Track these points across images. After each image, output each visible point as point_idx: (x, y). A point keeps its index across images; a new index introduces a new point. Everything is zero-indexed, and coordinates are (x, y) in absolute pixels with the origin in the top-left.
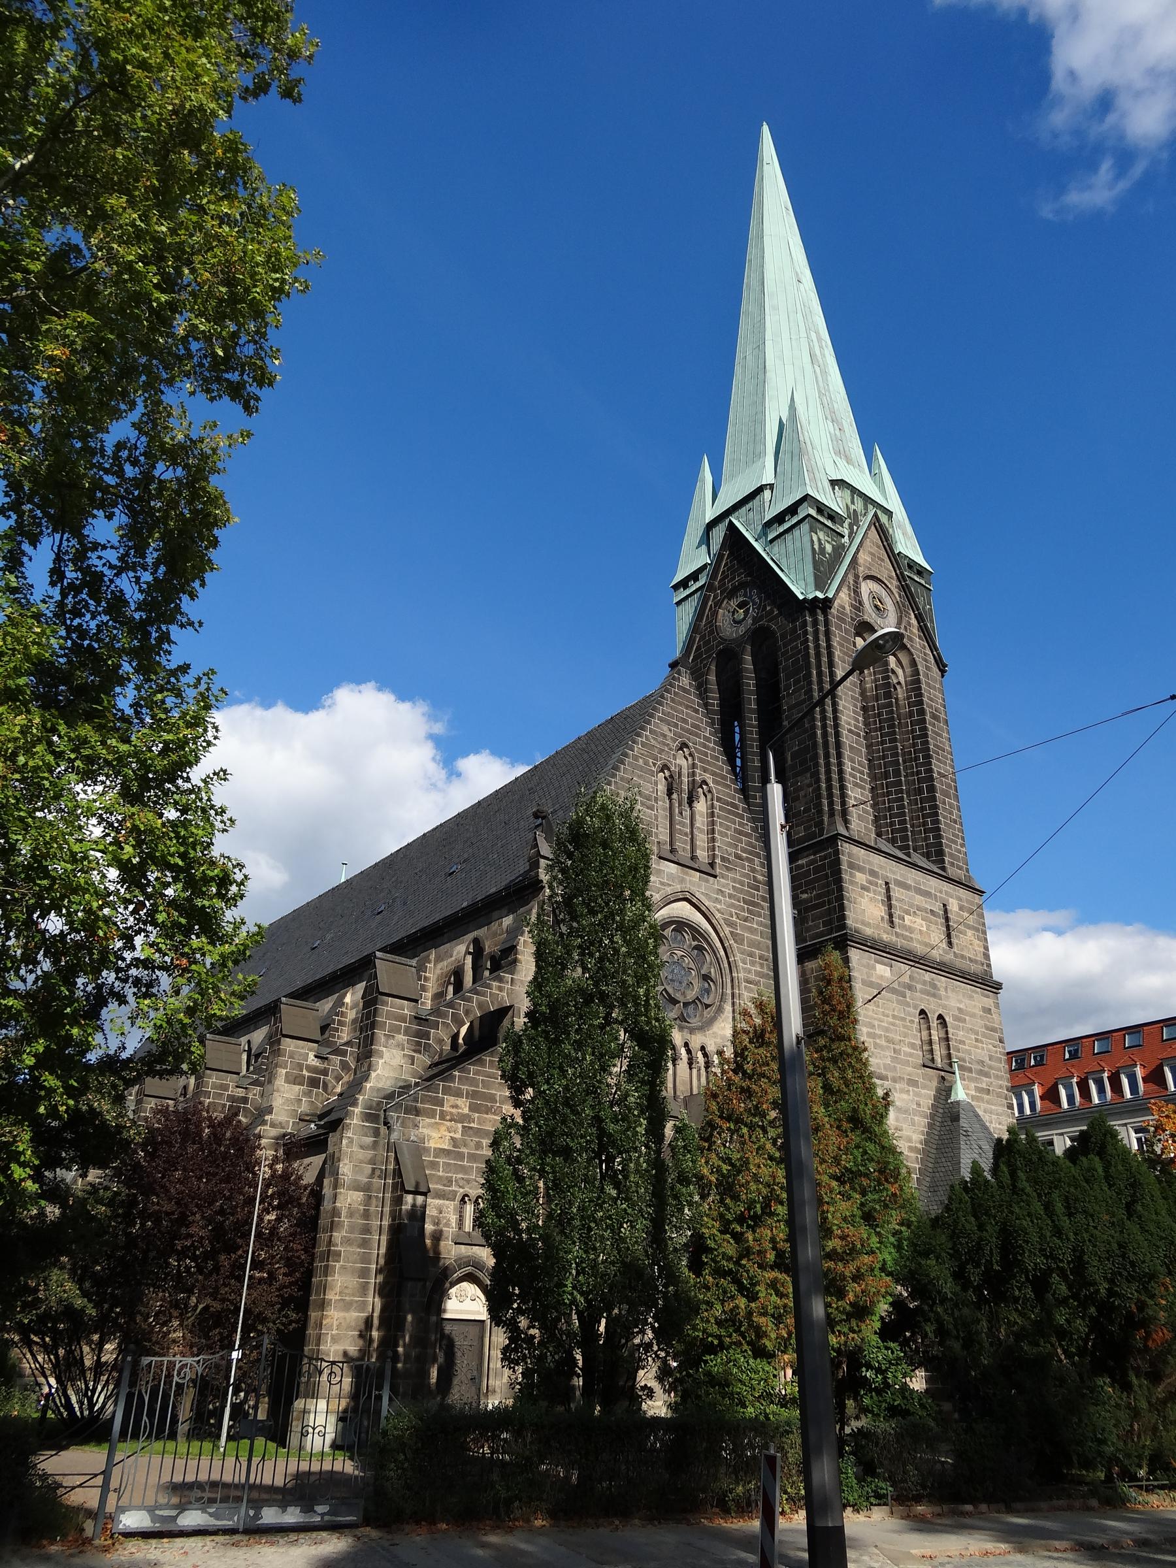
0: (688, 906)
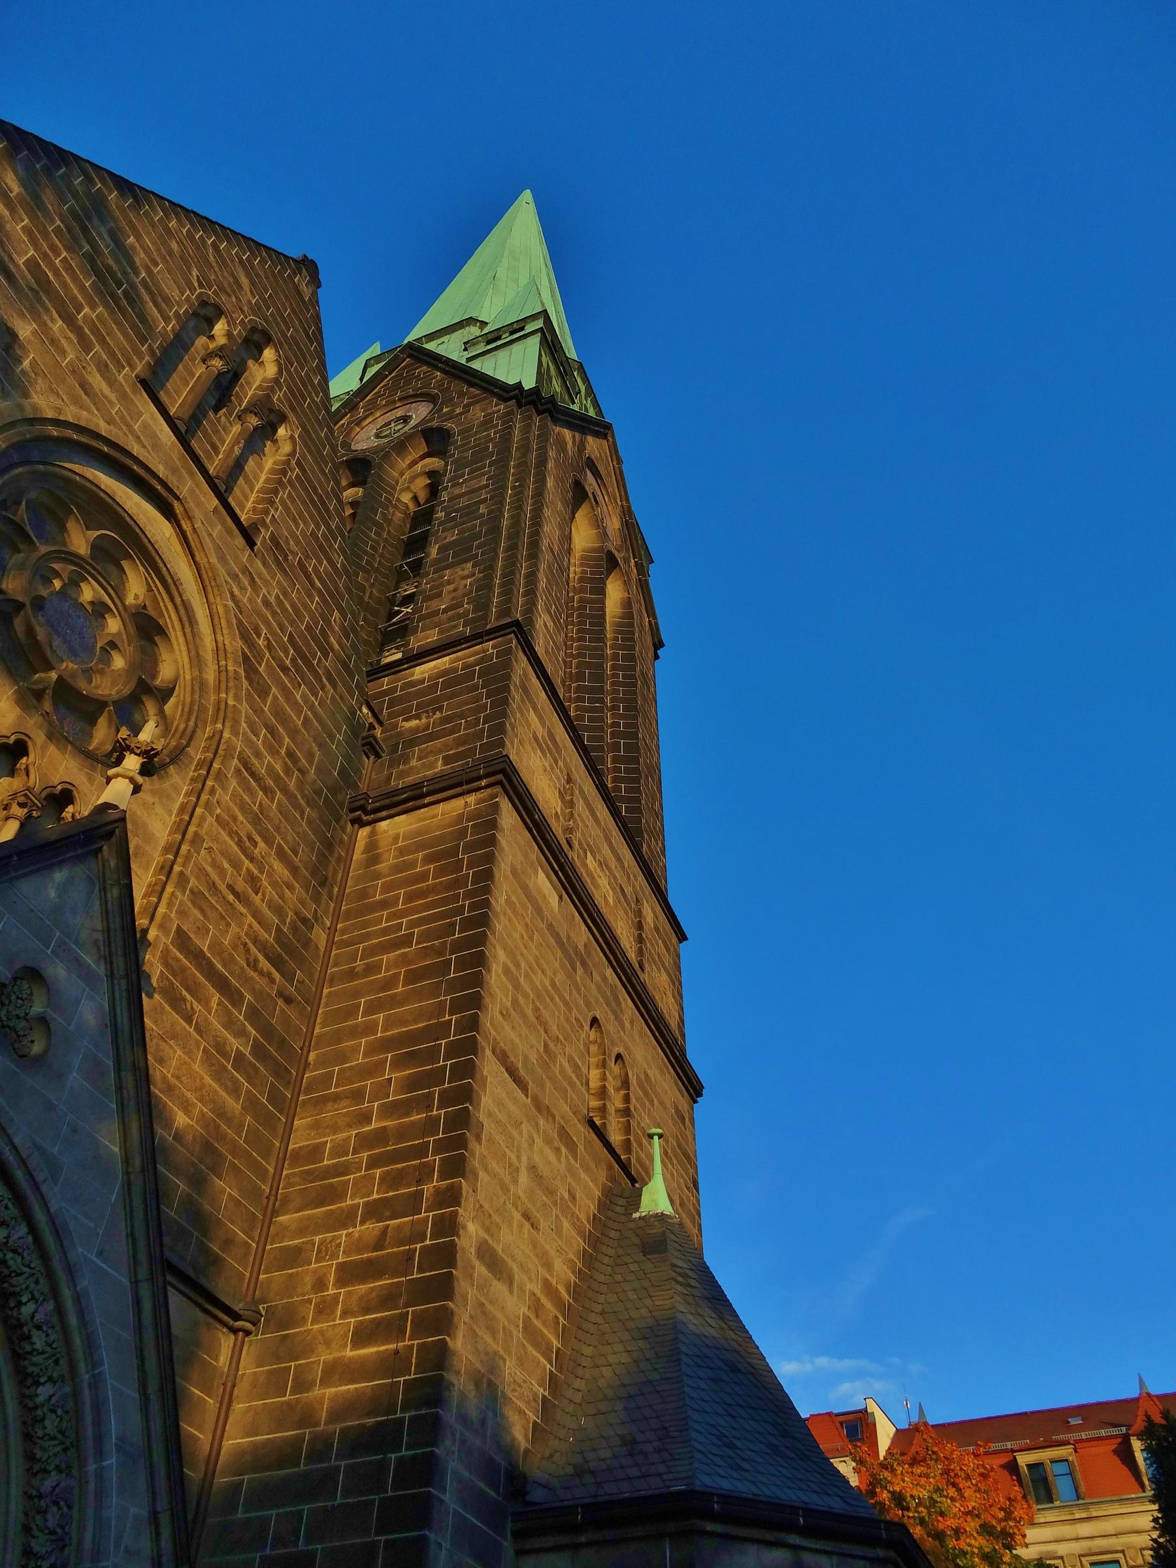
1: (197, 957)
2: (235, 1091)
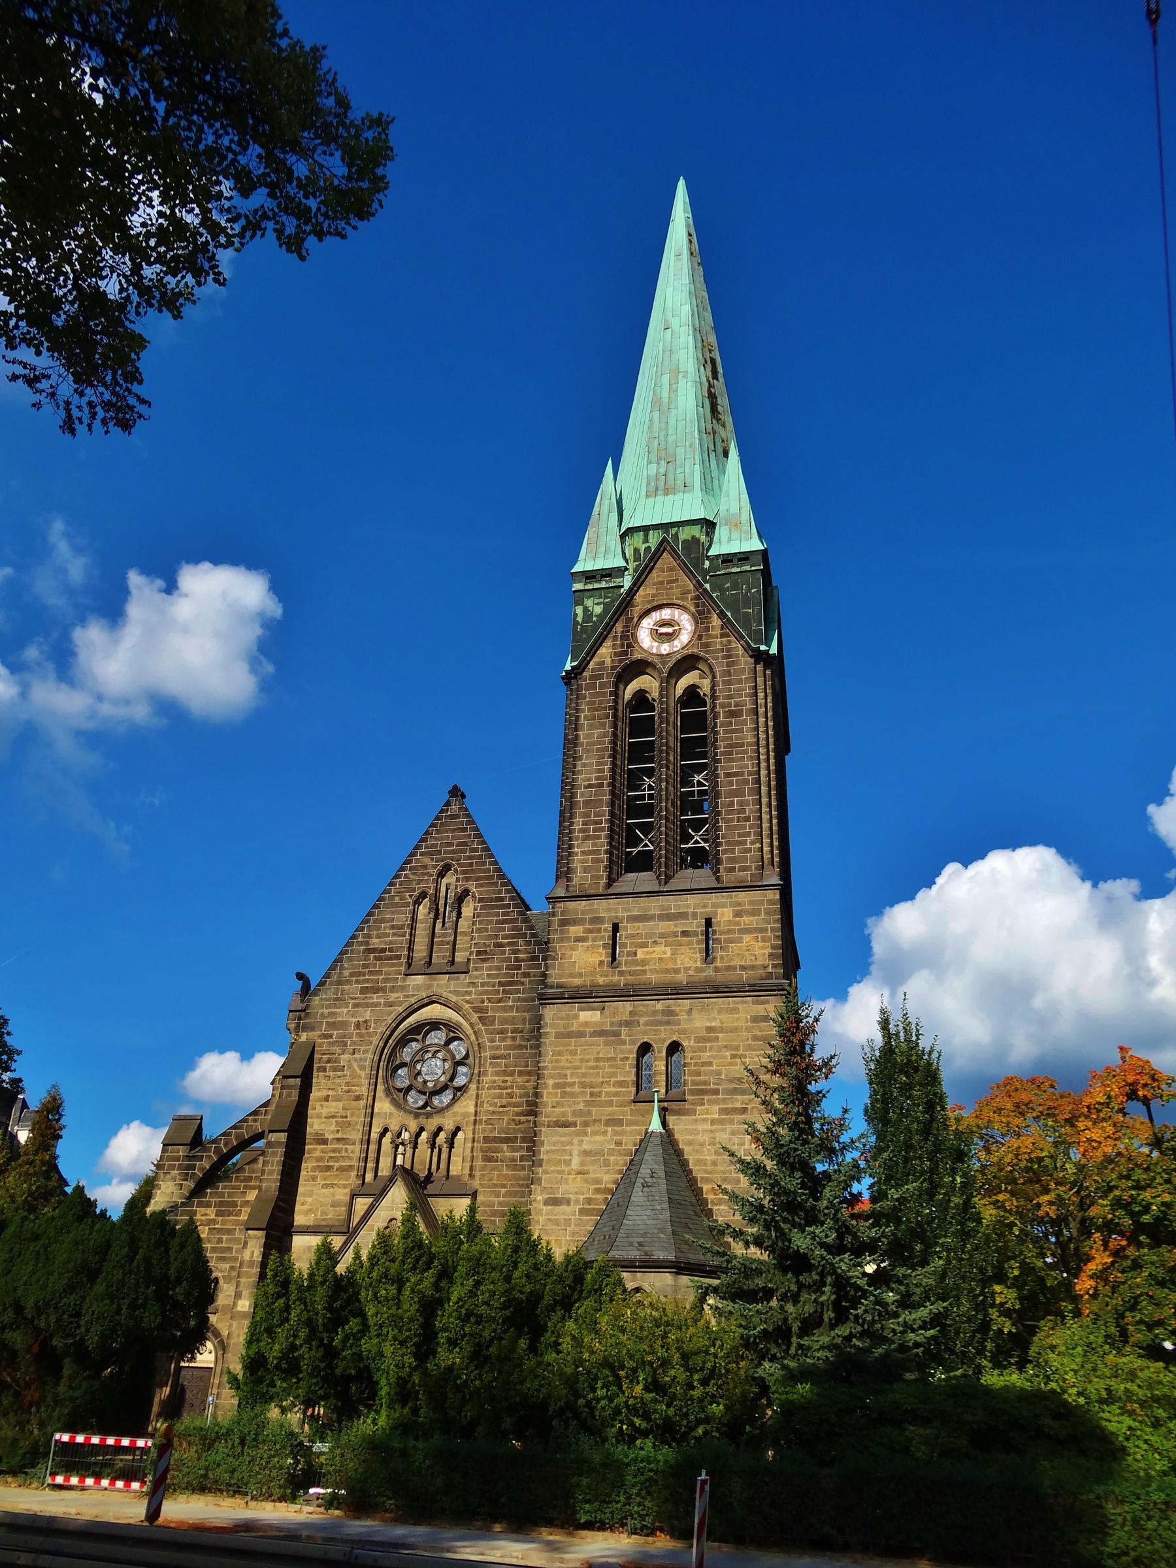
2: (523, 1168)
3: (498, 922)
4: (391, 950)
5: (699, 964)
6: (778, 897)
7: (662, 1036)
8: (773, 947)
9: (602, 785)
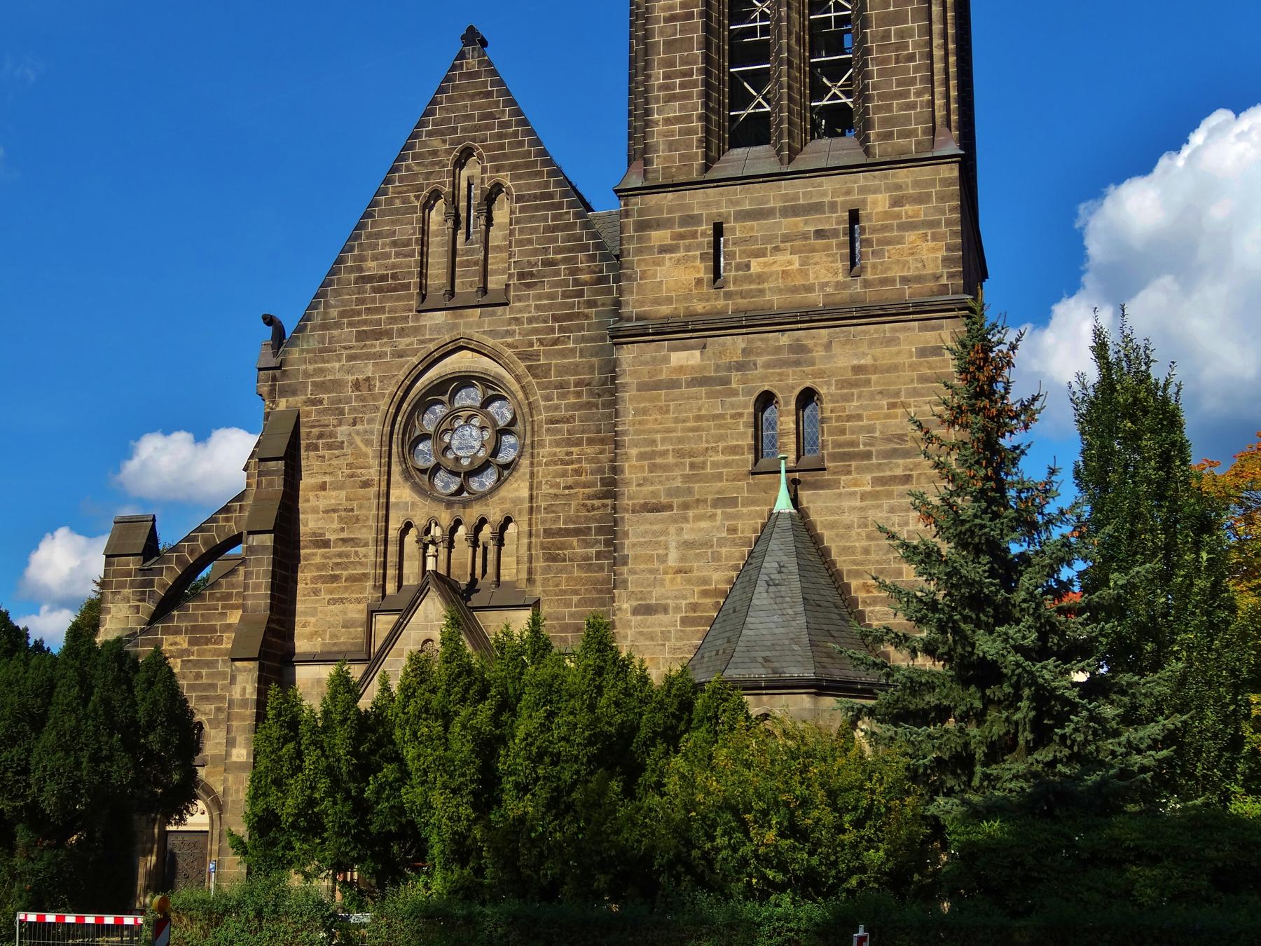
0: (469, 354)
1: (560, 533)
2: (601, 568)
3: (548, 229)
4: (394, 277)
5: (840, 278)
6: (956, 173)
7: (790, 381)
8: (949, 249)
9: (690, 16)
